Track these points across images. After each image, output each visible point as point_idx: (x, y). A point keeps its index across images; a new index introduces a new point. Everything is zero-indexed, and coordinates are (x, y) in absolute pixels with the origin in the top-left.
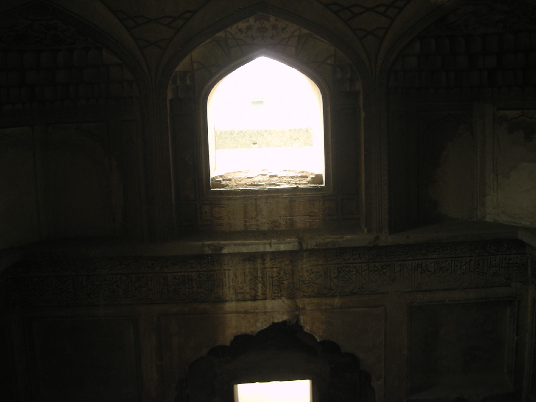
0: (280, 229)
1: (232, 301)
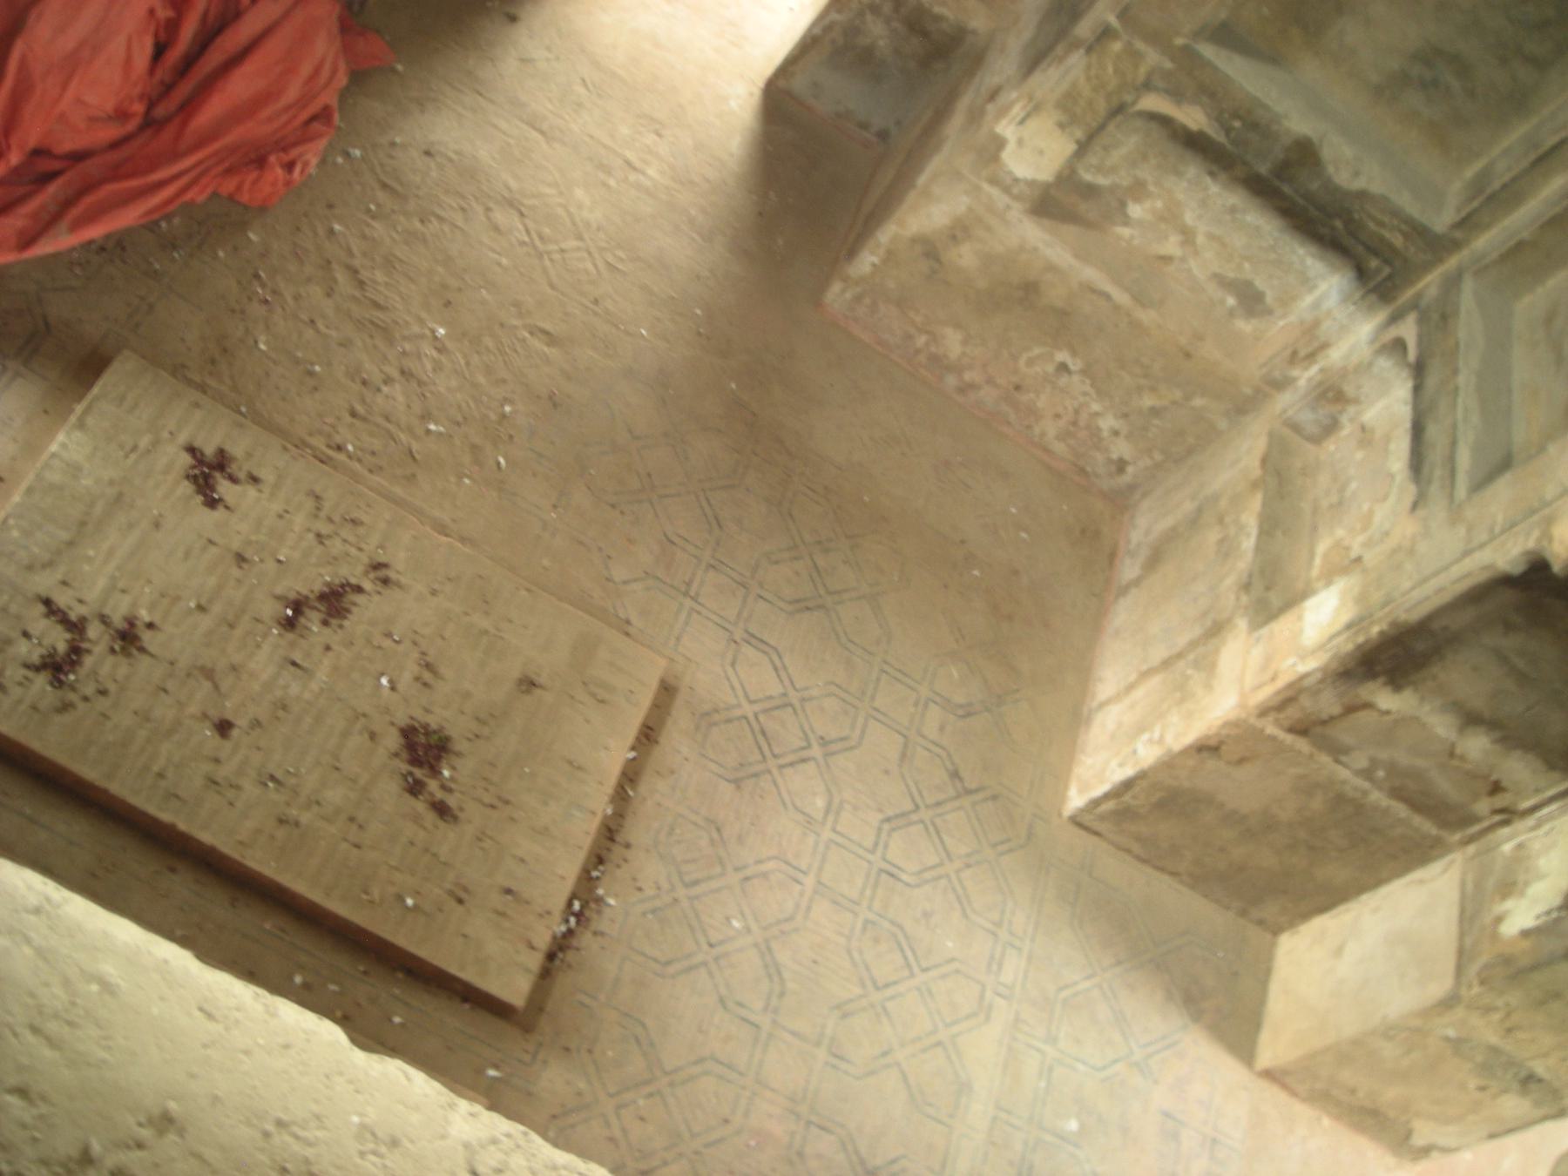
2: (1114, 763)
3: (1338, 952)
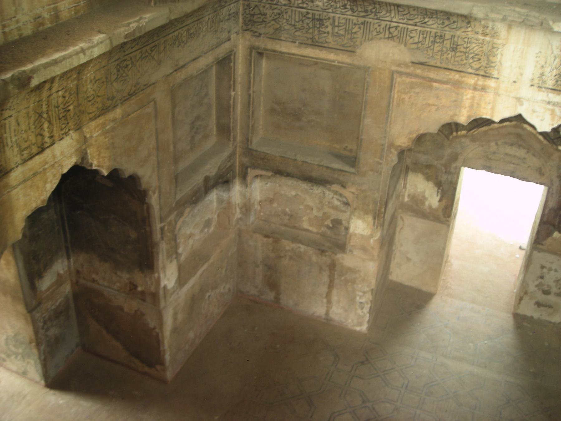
0: (46, 27)
1: (17, 167)
2: (359, 312)
3: (409, 260)
